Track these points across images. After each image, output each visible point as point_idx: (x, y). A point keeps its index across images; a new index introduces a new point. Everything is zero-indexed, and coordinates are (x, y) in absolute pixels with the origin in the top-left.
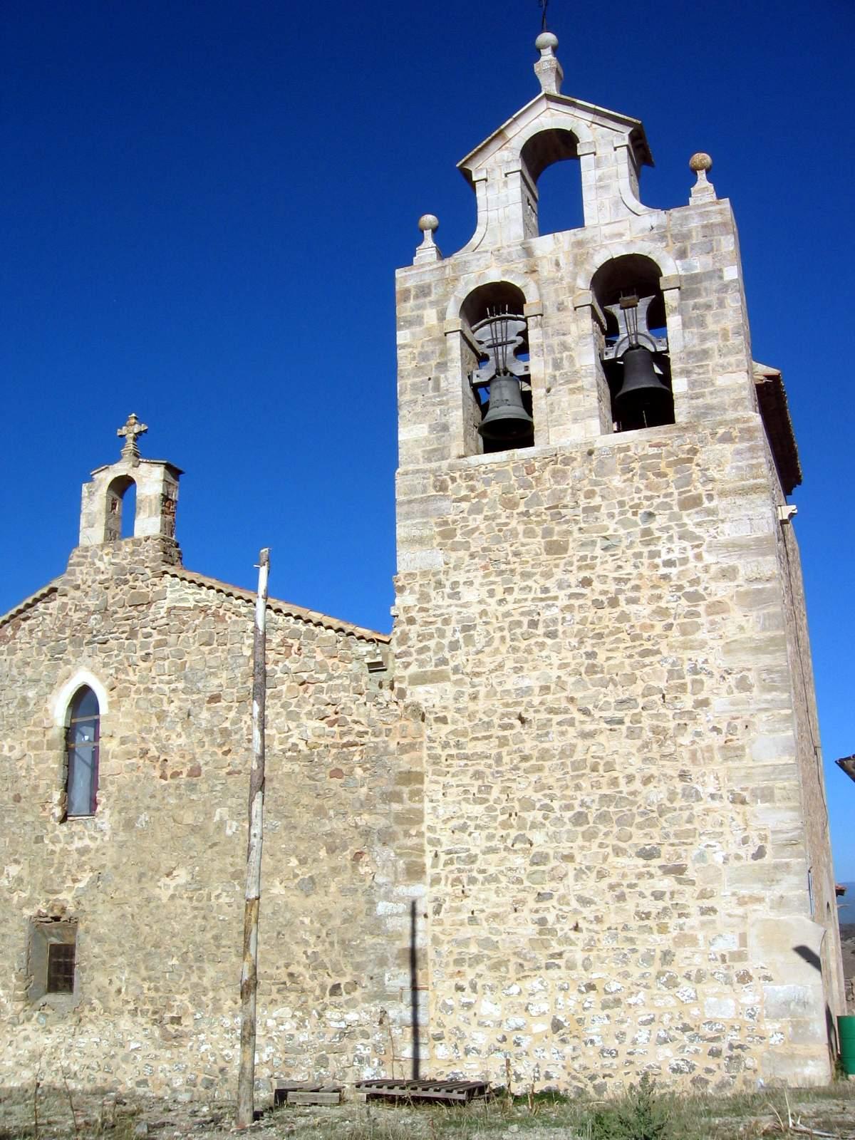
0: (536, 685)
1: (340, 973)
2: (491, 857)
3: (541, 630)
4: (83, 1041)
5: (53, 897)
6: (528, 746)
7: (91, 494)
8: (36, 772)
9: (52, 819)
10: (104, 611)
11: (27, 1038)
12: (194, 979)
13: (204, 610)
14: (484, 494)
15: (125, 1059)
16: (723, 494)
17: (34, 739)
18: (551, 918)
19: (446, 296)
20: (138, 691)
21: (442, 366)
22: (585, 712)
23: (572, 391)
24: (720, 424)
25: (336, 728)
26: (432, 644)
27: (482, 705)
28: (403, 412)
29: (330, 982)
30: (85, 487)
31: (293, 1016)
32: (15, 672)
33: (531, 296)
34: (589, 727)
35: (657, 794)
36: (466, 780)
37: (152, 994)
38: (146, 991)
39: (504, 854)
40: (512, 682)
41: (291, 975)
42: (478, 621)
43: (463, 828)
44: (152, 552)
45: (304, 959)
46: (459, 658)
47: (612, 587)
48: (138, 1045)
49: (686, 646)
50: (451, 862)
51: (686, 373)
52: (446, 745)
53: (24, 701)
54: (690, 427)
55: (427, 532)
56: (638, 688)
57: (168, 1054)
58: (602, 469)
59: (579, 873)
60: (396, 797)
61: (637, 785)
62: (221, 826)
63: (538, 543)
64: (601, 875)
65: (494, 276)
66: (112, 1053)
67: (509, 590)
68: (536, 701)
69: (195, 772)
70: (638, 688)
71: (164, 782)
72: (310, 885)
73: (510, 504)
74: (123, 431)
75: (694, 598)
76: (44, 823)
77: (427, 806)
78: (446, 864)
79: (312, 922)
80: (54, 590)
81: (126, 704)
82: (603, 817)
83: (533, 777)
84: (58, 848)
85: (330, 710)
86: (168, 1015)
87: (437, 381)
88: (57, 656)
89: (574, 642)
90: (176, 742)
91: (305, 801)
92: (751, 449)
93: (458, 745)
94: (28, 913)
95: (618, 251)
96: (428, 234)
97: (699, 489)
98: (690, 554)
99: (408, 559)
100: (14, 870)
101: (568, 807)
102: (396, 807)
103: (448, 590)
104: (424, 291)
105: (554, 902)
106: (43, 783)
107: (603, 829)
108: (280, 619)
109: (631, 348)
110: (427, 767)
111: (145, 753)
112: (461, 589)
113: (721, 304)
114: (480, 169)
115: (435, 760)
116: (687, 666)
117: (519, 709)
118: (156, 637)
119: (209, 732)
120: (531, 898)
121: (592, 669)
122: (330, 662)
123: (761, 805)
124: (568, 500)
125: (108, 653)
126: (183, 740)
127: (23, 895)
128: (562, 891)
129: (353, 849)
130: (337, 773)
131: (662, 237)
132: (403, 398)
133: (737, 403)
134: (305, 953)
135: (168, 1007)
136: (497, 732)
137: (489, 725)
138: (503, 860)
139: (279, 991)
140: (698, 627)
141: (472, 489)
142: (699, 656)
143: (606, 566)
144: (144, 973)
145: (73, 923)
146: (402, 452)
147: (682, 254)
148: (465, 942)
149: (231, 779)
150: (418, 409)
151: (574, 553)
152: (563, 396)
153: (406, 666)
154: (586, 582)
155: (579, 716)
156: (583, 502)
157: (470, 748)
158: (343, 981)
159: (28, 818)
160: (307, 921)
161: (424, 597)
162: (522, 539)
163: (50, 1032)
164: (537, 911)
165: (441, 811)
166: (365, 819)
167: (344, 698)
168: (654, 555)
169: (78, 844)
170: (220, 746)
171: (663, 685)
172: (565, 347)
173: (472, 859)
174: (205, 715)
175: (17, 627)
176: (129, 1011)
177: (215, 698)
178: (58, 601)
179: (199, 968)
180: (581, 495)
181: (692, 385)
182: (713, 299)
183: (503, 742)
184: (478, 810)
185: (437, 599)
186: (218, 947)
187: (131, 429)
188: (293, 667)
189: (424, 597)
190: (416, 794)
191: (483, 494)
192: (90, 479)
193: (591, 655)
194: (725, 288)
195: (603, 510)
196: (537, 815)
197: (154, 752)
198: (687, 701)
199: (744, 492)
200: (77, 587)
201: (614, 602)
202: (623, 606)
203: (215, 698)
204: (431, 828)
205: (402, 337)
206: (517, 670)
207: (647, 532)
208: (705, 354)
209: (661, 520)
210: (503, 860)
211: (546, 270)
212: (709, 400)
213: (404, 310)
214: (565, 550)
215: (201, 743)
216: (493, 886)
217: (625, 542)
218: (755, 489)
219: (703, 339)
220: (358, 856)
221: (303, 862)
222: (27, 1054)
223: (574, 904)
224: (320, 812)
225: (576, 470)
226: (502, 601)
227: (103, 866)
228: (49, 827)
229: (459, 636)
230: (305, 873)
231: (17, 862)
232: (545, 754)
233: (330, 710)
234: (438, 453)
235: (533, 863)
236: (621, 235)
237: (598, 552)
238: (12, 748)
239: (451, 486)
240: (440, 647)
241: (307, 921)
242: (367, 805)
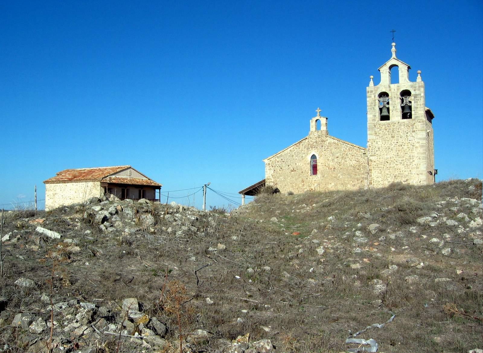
0: (389, 157)
3: (390, 149)
7: (312, 122)
8: (305, 168)
10: (316, 142)
13: (335, 143)
14: (382, 128)
16: (418, 130)
17: (305, 163)
19: (375, 93)
21: (375, 105)
22: (397, 161)
23: (396, 112)
24: (419, 119)
25: (358, 162)
26: (373, 150)
27: (381, 160)
28: (368, 113)
30: (311, 121)
32: (300, 152)
33: (390, 95)
34: (397, 164)
35: (406, 173)
36: (378, 171)
40: (386, 157)
42: (381, 147)
43: (378, 177)
44: (324, 133)
46: (377, 153)
47: (401, 143)
49: (412, 153)
51: (414, 110)
52: (375, 165)
53: (302, 157)
54: (414, 120)
55: (372, 133)
56: (404, 158)
58: (400, 125)
61: (404, 172)
62: (339, 177)
63: (390, 136)
65: (384, 90)
67: (385, 143)
68: (389, 160)
69: (334, 168)
70: (404, 158)
73: (386, 130)
74: (317, 111)
77: (372, 174)
80: (306, 138)
81: (322, 158)
84: (310, 180)
85: (357, 160)
87: (374, 108)
89: (395, 151)
90: (331, 164)
91: (353, 173)
92: (423, 124)
93: (377, 165)
95: (404, 89)
96: (371, 79)
97: (415, 129)
98: (413, 139)
99: (369, 137)
103: (376, 142)
104: (372, 92)
106: (307, 170)
108: (348, 145)
109: (406, 105)
110: (372, 169)
111: (325, 165)
112: (378, 142)
113: (420, 99)
114: (381, 70)
115: (374, 168)
116: (412, 156)
117: (387, 161)
118: (326, 147)
119: (337, 162)
121: (398, 155)
122: (357, 152)
123: (421, 175)
124: (395, 130)
126: (332, 164)
129: (361, 180)
130: (358, 169)
131: (412, 87)
132: (368, 110)
133: (422, 116)
136: (383, 164)
137: (382, 163)
140: (413, 150)
141: (380, 127)
142: (414, 154)
143: (400, 140)
146: (368, 120)
147: (415, 90)
149: (341, 170)
150: (371, 112)
151: (396, 138)
152: (394, 112)
154: (397, 142)
155: (396, 162)
156: (397, 130)
161: (372, 143)
162: (388, 135)
166: (363, 176)
167: (359, 158)
168: (407, 139)
169: (314, 179)
171: (408, 158)
172: (395, 104)
173: (379, 182)
174: (336, 160)
175: (299, 144)
177: (337, 157)
178: (307, 141)
180: (397, 129)
181: (415, 112)
182: (419, 99)
183: (384, 165)
184: (380, 175)
185: (374, 144)
187: (318, 111)
188: (351, 153)
189: (372, 143)
191: (382, 128)
192: (311, 119)
193: (398, 153)
194: (421, 97)
195: (400, 132)
196: (389, 176)
197: (327, 165)
198: (411, 160)
199: (422, 130)
200: (311, 138)
201: (401, 146)
202: (403, 146)
203: (337, 157)
205: (368, 99)
206: (387, 155)
207: (407, 135)
208: (417, 108)
209: (409, 134)
211: (392, 90)
212: (417, 115)
213: (368, 95)
214: (394, 137)
215: (335, 164)
217: (404, 137)
218: (423, 130)
219: (417, 105)
220: (362, 181)
221: (353, 182)
224: (356, 175)
225: (396, 125)
226: (384, 145)
229: (378, 149)
230: (353, 184)
232: (390, 167)
233: (357, 160)
234: (374, 120)
236: (405, 86)
237: (399, 138)
239: (376, 126)
240: (374, 151)
242: (363, 174)
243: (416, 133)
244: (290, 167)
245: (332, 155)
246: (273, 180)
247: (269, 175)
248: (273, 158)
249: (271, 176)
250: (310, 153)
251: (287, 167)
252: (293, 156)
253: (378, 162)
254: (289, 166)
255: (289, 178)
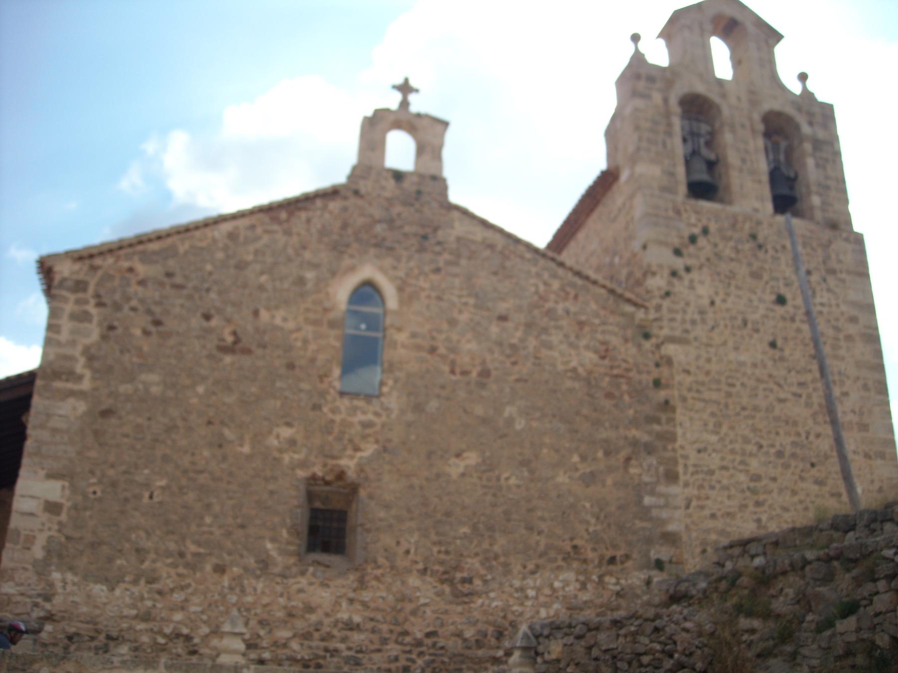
1: (615, 547)
2: (724, 472)
4: (366, 596)
5: (331, 462)
6: (745, 401)
8: (312, 347)
9: (332, 391)
10: (390, 222)
11: (300, 591)
12: (486, 545)
13: (491, 247)
15: (414, 613)
16: (849, 272)
17: (311, 316)
18: (764, 518)
20: (429, 297)
21: (669, 133)
22: (779, 385)
26: (679, 317)
29: (609, 554)
31: (577, 580)
32: (290, 251)
34: (782, 395)
37: (443, 556)
38: (435, 554)
39: (732, 471)
40: (732, 356)
41: (575, 547)
45: (586, 536)
46: (699, 331)
48: (427, 601)
50: (697, 472)
53: (301, 281)
57: (459, 609)
59: (781, 491)
60: (658, 421)
62: (510, 421)
64: (794, 493)
66: (399, 607)
69: (485, 373)
71: (453, 378)
72: (590, 479)
75: (837, 329)
76: (323, 394)
77: (679, 431)
78: (692, 474)
79: (592, 506)
82: (794, 455)
83: (750, 422)
86: (459, 575)
88: (339, 248)
91: (585, 411)
93: (698, 391)
94: (301, 473)
100: (286, 432)
101: (772, 446)
102: (656, 428)
105: (766, 508)
106: (322, 357)
107: (793, 463)
119: (500, 344)
120: (751, 504)
125: (398, 259)
127: (296, 456)
128: (770, 502)
129: (623, 454)
130: (609, 395)
134: (587, 530)
135: (457, 568)
137: (718, 382)
138: (732, 476)
139: (564, 559)
144: (434, 538)
145: (354, 489)
147: (811, 124)
148: (708, 531)
153: (661, 328)
155: (775, 388)
157: (707, 395)
158: (619, 554)
159: (305, 386)
160: (588, 505)
163: (328, 586)
164: (755, 513)
165: (688, 435)
166: (634, 433)
169: (360, 417)
170: (508, 356)
173: (711, 472)
175: (291, 214)
176: (418, 571)
179: (490, 537)
184: (714, 438)
186: (509, 520)
190: (671, 420)
196: (754, 449)
197: (442, 350)
203: (503, 318)
204: (682, 447)
206: (736, 349)
210: (732, 476)
215: (491, 351)
216: (726, 493)
220: (628, 460)
221: (583, 458)
222: (301, 605)
223: (779, 511)
227: (389, 441)
228: (329, 398)
229: (697, 317)
230: (585, 468)
231: (289, 425)
232: (756, 408)
235: (752, 480)
238: (285, 320)
240: (684, 321)
241: (588, 505)
242: (634, 423)
243: (843, 281)
244: (214, 323)
245: (472, 301)
246: (86, 385)
247: (68, 351)
248: (110, 260)
249: (82, 361)
250: (352, 269)
251: (196, 322)
252: (241, 266)
253: (702, 377)
254: (207, 317)
255: (201, 389)
